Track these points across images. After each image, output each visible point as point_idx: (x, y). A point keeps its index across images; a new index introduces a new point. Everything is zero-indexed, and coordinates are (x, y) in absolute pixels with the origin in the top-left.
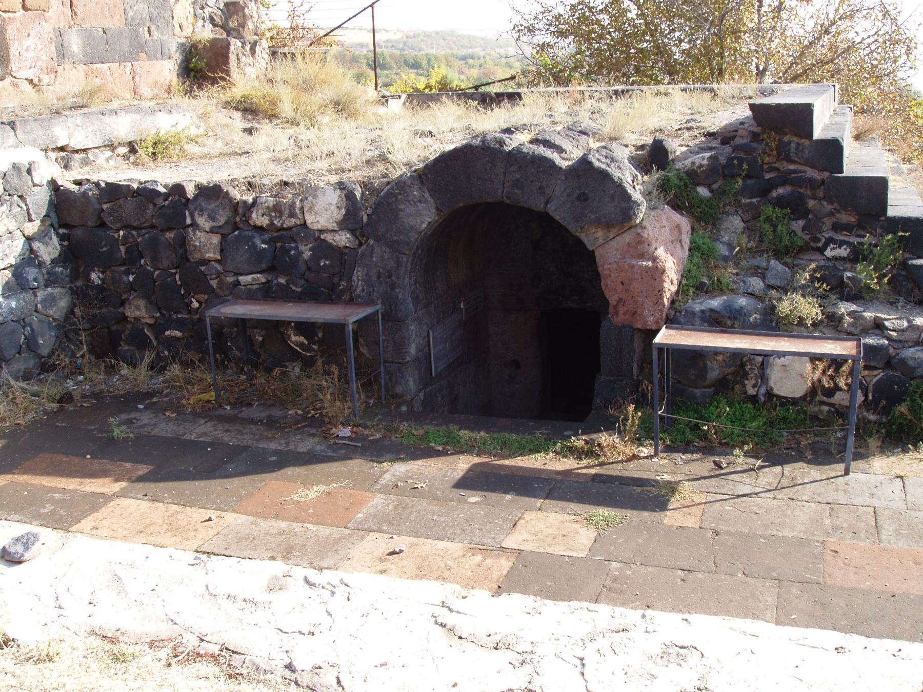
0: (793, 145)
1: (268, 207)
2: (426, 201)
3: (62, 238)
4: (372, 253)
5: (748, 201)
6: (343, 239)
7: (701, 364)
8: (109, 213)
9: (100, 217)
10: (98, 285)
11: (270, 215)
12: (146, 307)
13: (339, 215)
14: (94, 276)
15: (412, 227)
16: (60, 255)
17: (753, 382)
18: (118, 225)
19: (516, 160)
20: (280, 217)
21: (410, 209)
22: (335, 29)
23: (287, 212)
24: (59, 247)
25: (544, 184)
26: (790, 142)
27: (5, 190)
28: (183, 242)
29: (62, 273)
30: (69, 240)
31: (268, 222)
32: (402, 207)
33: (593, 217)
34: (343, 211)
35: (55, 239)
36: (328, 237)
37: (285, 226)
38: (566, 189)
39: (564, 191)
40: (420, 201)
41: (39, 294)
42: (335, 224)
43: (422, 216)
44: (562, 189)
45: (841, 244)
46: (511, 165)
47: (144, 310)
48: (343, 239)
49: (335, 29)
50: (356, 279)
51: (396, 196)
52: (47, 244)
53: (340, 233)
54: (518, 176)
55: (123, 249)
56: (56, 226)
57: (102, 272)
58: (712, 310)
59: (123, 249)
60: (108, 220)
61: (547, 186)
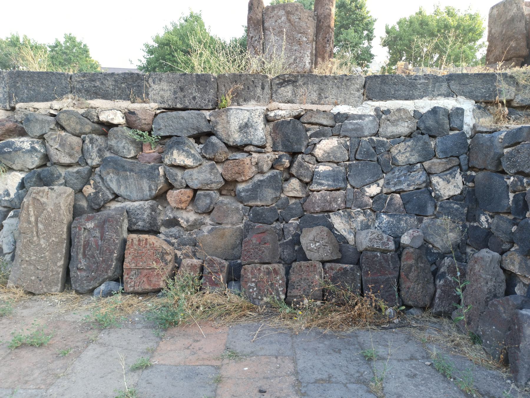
3: (467, 179)
8: (508, 158)
9: (500, 163)
10: (485, 228)
12: (520, 264)
14: (483, 218)
16: (461, 193)
18: (513, 171)
24: (461, 186)
27: (418, 128)
29: (457, 210)
30: (473, 181)
35: (459, 179)
41: (424, 221)
47: (517, 267)
52: (449, 182)
55: (511, 196)
56: (464, 168)
57: (492, 217)
59: (511, 196)
60: (505, 165)
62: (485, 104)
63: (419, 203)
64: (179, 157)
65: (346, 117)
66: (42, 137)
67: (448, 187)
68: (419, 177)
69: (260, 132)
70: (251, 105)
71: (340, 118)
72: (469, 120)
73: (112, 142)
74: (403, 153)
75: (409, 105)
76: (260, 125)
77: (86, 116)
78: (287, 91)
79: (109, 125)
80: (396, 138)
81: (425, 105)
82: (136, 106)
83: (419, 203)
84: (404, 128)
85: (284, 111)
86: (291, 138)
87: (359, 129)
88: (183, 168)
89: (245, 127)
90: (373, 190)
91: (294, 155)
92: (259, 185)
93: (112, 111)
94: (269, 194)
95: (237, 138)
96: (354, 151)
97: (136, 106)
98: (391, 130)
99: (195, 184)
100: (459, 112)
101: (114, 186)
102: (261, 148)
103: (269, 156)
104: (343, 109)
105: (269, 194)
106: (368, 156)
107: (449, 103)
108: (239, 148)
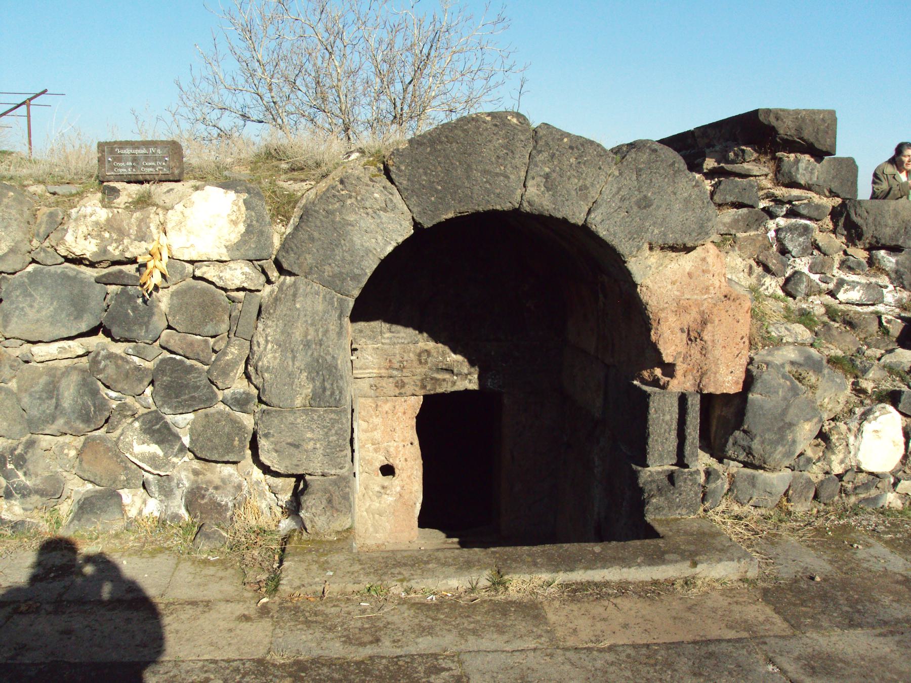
0: (802, 165)
1: (97, 223)
2: (395, 207)
4: (295, 295)
5: (745, 234)
6: (237, 274)
7: (790, 437)
11: (99, 236)
13: (235, 233)
15: (368, 251)
17: (841, 456)
19: (547, 144)
20: (119, 241)
21: (368, 222)
22: (37, 95)
23: (133, 231)
25: (588, 183)
26: (797, 161)
31: (96, 249)
32: (351, 218)
33: (656, 231)
34: (242, 228)
36: (210, 272)
37: (128, 255)
38: (620, 189)
39: (618, 193)
40: (385, 210)
42: (225, 250)
44: (614, 190)
45: (853, 285)
46: (540, 152)
48: (237, 274)
49: (37, 95)
50: (262, 341)
51: (342, 200)
53: (232, 264)
54: (547, 170)
58: (792, 363)
61: (592, 185)
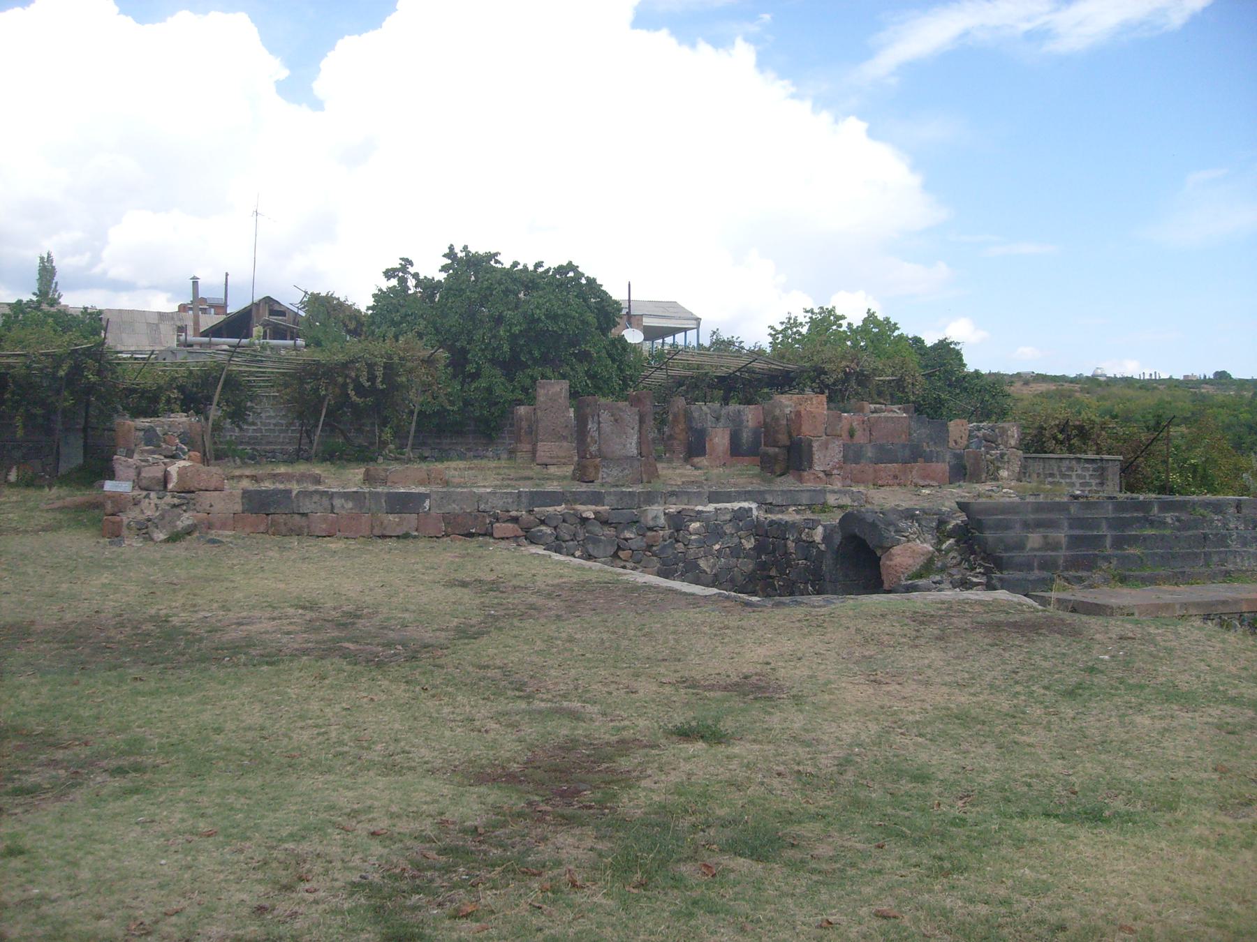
6: (823, 547)
28: (785, 545)
43: (837, 539)
62: (761, 504)
63: (736, 551)
64: (628, 535)
65: (702, 512)
66: (555, 528)
67: (749, 544)
68: (736, 540)
69: (662, 521)
70: (655, 507)
71: (700, 512)
72: (755, 513)
73: (590, 528)
74: (728, 529)
75: (728, 505)
76: (663, 517)
77: (574, 515)
78: (673, 499)
79: (587, 519)
80: (726, 522)
81: (736, 505)
82: (599, 508)
83: (736, 551)
84: (728, 517)
85: (673, 509)
86: (678, 522)
87: (708, 518)
88: (626, 540)
89: (656, 517)
90: (717, 547)
91: (678, 531)
92: (665, 546)
93: (588, 511)
94: (670, 551)
95: (651, 524)
96: (707, 527)
97: (599, 508)
98: (723, 518)
99: (634, 547)
100: (751, 509)
101: (591, 552)
102: (663, 528)
103: (667, 532)
104: (700, 508)
105: (670, 551)
106: (713, 531)
107: (745, 505)
108: (651, 529)
